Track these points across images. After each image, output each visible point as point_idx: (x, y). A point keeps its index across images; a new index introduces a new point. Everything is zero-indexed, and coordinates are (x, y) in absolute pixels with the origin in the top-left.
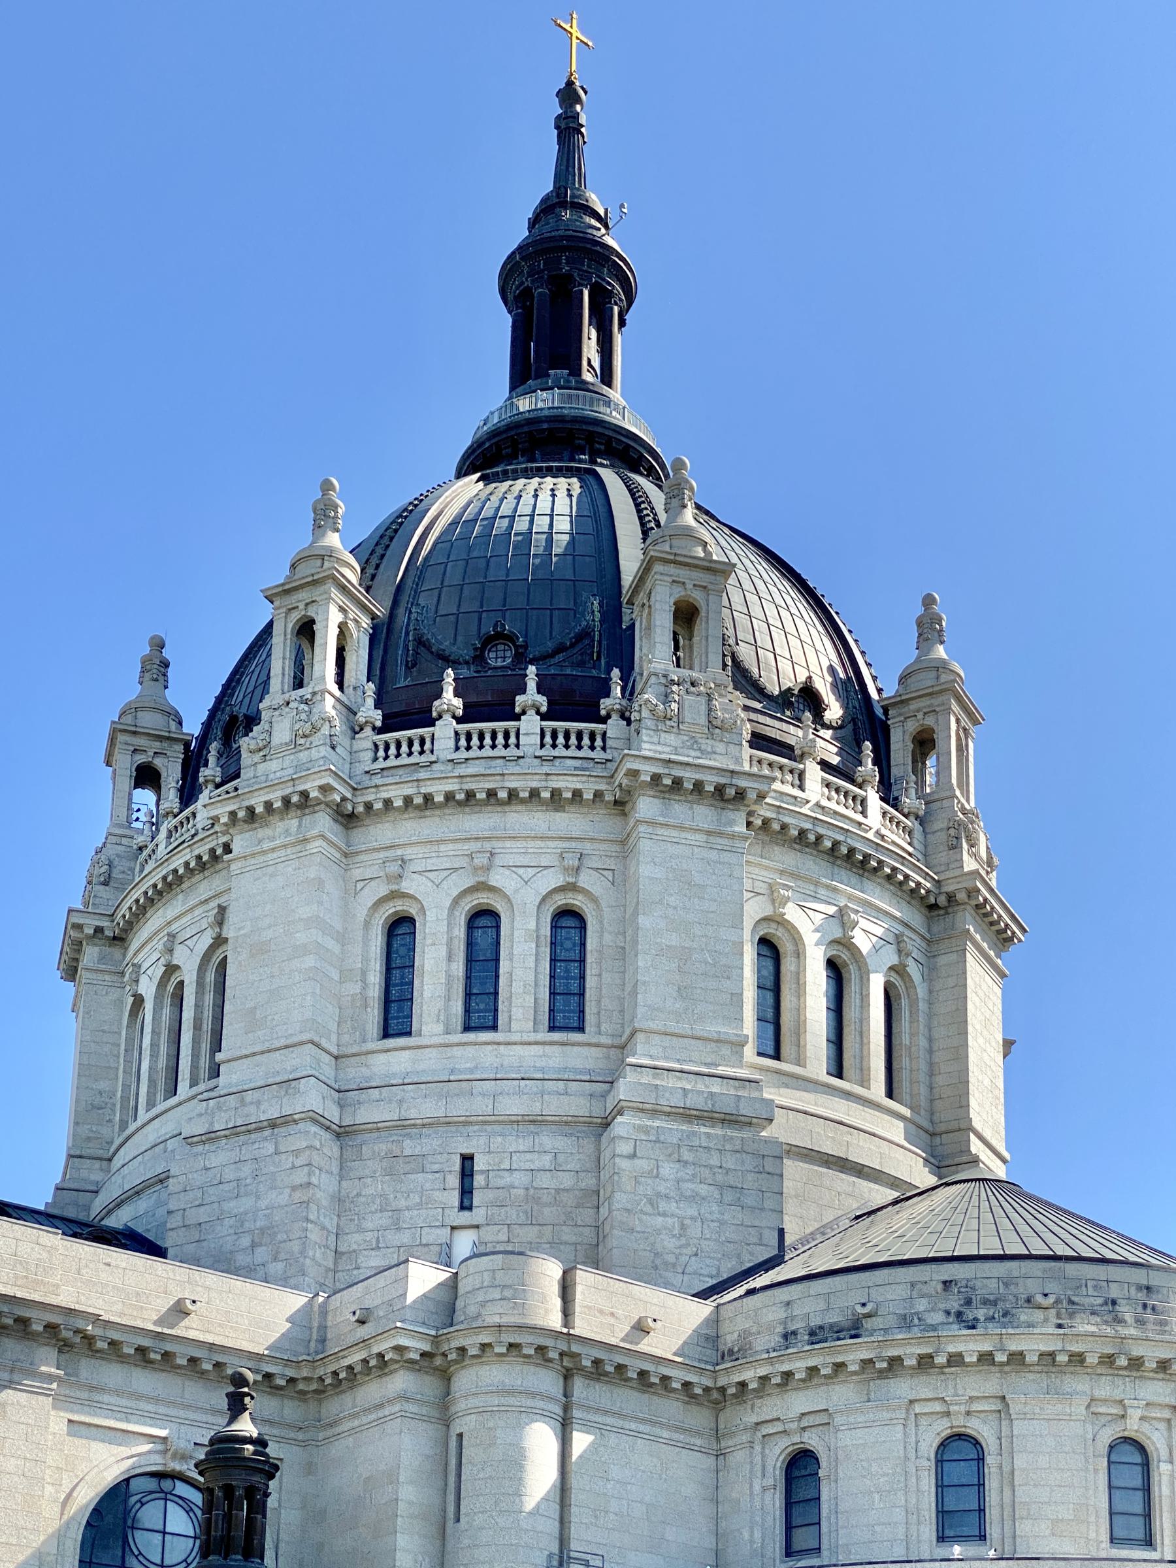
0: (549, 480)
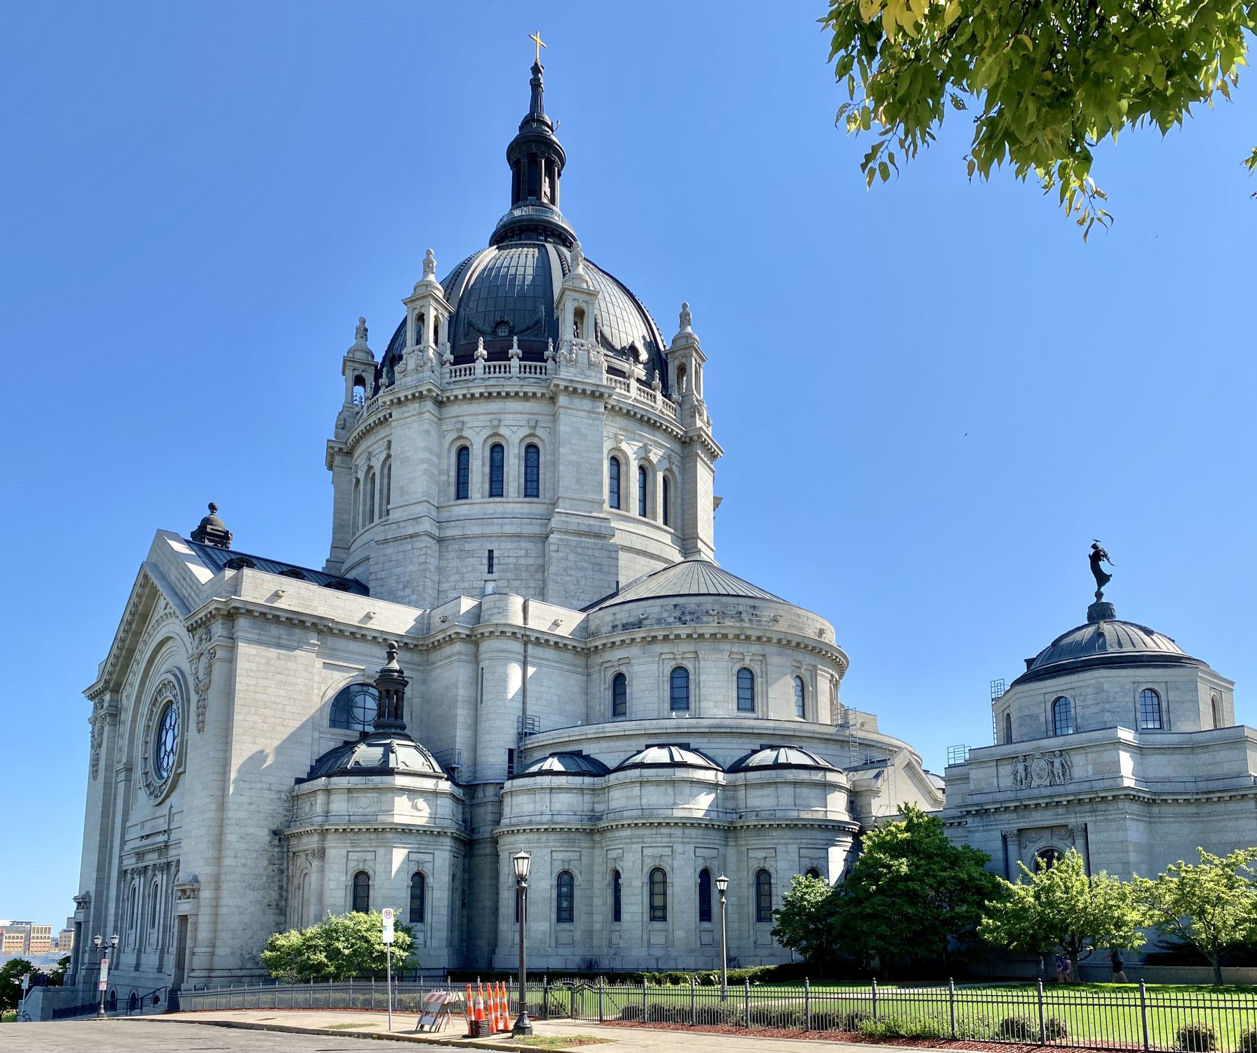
0: (525, 249)
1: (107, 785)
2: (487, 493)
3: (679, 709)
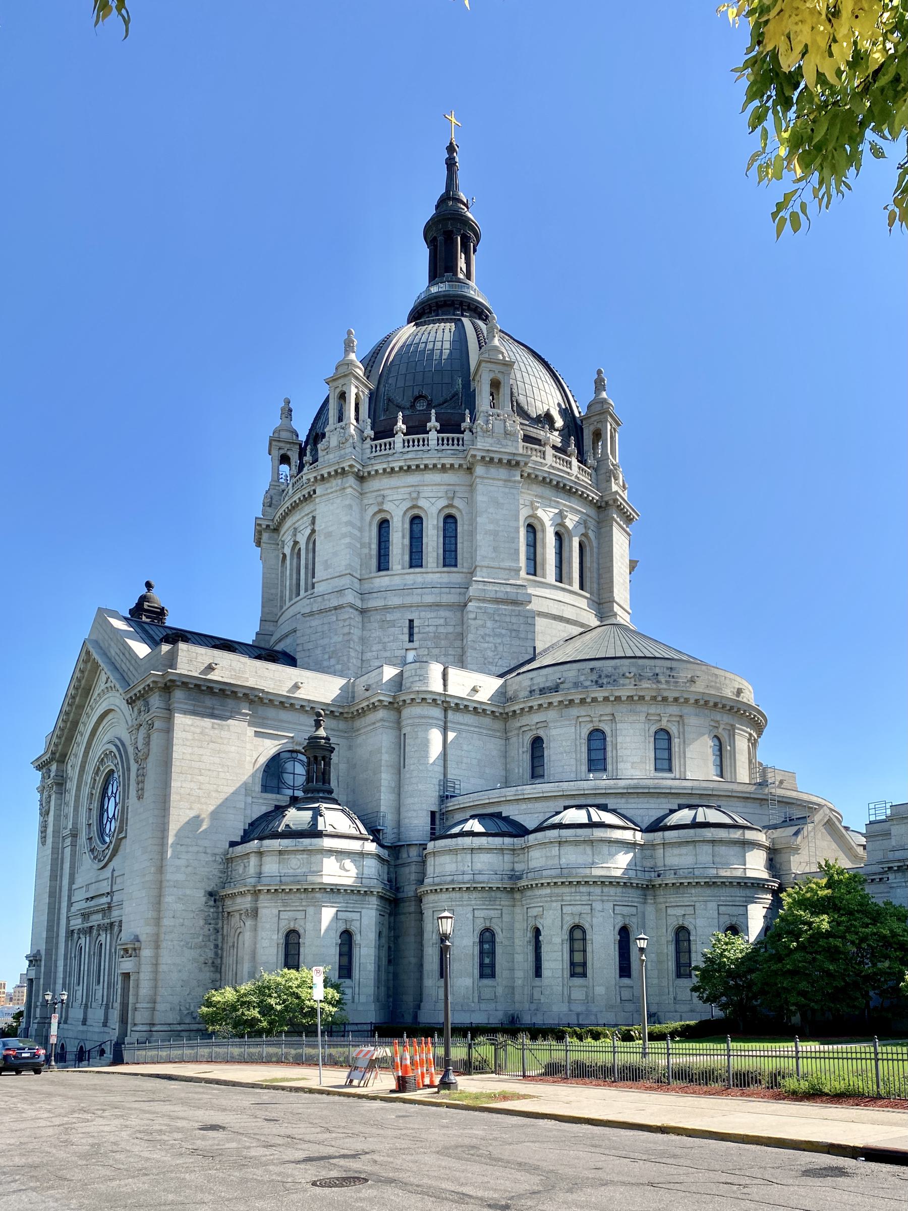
1: (55, 850)
2: (407, 564)
3: (596, 770)
